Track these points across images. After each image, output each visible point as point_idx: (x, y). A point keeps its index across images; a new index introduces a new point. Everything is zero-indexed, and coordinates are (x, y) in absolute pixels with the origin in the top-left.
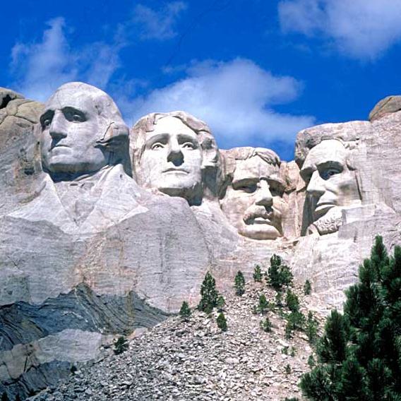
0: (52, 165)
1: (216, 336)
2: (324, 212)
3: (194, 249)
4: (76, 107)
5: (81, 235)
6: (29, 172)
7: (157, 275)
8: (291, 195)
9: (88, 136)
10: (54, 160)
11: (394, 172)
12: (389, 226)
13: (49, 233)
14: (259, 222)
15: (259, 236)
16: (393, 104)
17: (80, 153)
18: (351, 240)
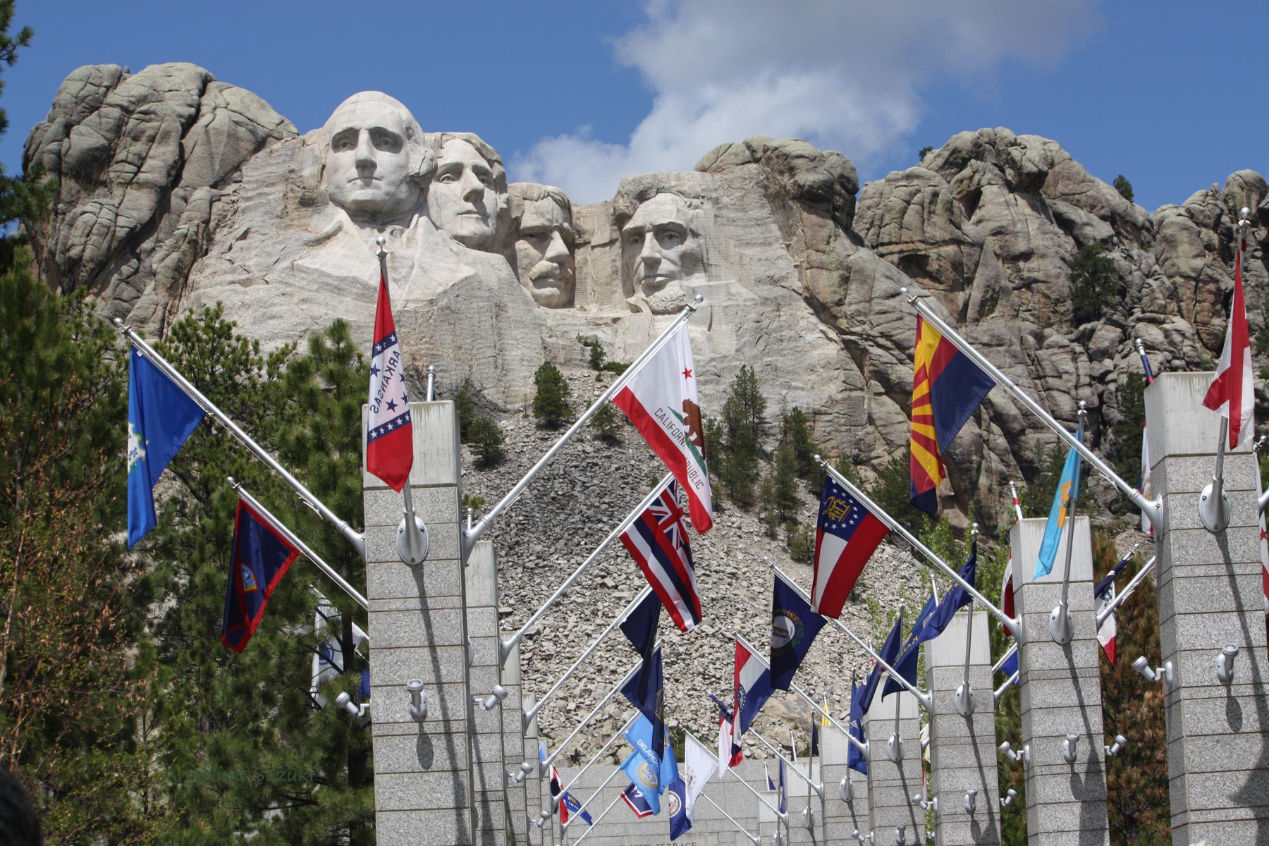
0: (356, 202)
1: (607, 453)
2: (660, 287)
3: (525, 326)
4: (390, 129)
5: (408, 301)
6: (308, 202)
7: (491, 359)
8: (582, 250)
9: (403, 167)
10: (359, 194)
11: (748, 244)
12: (754, 316)
13: (363, 295)
14: (552, 286)
15: (549, 303)
16: (736, 155)
17: (392, 189)
18: (705, 329)
